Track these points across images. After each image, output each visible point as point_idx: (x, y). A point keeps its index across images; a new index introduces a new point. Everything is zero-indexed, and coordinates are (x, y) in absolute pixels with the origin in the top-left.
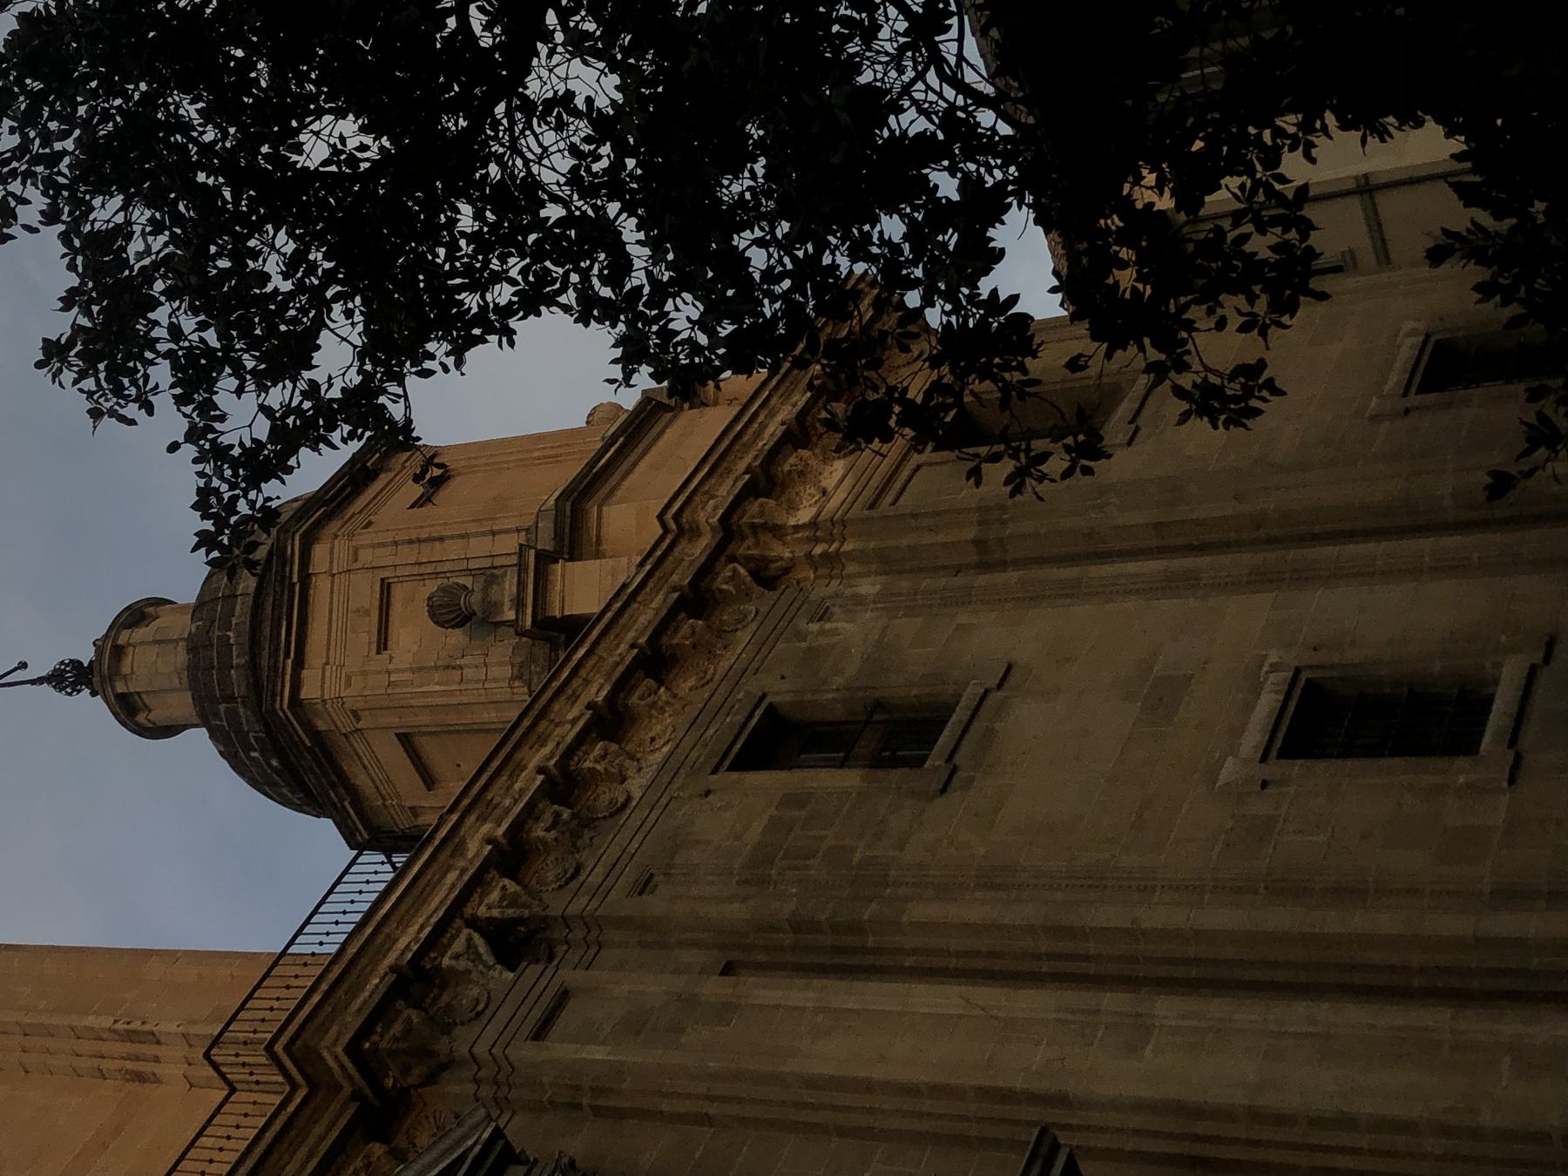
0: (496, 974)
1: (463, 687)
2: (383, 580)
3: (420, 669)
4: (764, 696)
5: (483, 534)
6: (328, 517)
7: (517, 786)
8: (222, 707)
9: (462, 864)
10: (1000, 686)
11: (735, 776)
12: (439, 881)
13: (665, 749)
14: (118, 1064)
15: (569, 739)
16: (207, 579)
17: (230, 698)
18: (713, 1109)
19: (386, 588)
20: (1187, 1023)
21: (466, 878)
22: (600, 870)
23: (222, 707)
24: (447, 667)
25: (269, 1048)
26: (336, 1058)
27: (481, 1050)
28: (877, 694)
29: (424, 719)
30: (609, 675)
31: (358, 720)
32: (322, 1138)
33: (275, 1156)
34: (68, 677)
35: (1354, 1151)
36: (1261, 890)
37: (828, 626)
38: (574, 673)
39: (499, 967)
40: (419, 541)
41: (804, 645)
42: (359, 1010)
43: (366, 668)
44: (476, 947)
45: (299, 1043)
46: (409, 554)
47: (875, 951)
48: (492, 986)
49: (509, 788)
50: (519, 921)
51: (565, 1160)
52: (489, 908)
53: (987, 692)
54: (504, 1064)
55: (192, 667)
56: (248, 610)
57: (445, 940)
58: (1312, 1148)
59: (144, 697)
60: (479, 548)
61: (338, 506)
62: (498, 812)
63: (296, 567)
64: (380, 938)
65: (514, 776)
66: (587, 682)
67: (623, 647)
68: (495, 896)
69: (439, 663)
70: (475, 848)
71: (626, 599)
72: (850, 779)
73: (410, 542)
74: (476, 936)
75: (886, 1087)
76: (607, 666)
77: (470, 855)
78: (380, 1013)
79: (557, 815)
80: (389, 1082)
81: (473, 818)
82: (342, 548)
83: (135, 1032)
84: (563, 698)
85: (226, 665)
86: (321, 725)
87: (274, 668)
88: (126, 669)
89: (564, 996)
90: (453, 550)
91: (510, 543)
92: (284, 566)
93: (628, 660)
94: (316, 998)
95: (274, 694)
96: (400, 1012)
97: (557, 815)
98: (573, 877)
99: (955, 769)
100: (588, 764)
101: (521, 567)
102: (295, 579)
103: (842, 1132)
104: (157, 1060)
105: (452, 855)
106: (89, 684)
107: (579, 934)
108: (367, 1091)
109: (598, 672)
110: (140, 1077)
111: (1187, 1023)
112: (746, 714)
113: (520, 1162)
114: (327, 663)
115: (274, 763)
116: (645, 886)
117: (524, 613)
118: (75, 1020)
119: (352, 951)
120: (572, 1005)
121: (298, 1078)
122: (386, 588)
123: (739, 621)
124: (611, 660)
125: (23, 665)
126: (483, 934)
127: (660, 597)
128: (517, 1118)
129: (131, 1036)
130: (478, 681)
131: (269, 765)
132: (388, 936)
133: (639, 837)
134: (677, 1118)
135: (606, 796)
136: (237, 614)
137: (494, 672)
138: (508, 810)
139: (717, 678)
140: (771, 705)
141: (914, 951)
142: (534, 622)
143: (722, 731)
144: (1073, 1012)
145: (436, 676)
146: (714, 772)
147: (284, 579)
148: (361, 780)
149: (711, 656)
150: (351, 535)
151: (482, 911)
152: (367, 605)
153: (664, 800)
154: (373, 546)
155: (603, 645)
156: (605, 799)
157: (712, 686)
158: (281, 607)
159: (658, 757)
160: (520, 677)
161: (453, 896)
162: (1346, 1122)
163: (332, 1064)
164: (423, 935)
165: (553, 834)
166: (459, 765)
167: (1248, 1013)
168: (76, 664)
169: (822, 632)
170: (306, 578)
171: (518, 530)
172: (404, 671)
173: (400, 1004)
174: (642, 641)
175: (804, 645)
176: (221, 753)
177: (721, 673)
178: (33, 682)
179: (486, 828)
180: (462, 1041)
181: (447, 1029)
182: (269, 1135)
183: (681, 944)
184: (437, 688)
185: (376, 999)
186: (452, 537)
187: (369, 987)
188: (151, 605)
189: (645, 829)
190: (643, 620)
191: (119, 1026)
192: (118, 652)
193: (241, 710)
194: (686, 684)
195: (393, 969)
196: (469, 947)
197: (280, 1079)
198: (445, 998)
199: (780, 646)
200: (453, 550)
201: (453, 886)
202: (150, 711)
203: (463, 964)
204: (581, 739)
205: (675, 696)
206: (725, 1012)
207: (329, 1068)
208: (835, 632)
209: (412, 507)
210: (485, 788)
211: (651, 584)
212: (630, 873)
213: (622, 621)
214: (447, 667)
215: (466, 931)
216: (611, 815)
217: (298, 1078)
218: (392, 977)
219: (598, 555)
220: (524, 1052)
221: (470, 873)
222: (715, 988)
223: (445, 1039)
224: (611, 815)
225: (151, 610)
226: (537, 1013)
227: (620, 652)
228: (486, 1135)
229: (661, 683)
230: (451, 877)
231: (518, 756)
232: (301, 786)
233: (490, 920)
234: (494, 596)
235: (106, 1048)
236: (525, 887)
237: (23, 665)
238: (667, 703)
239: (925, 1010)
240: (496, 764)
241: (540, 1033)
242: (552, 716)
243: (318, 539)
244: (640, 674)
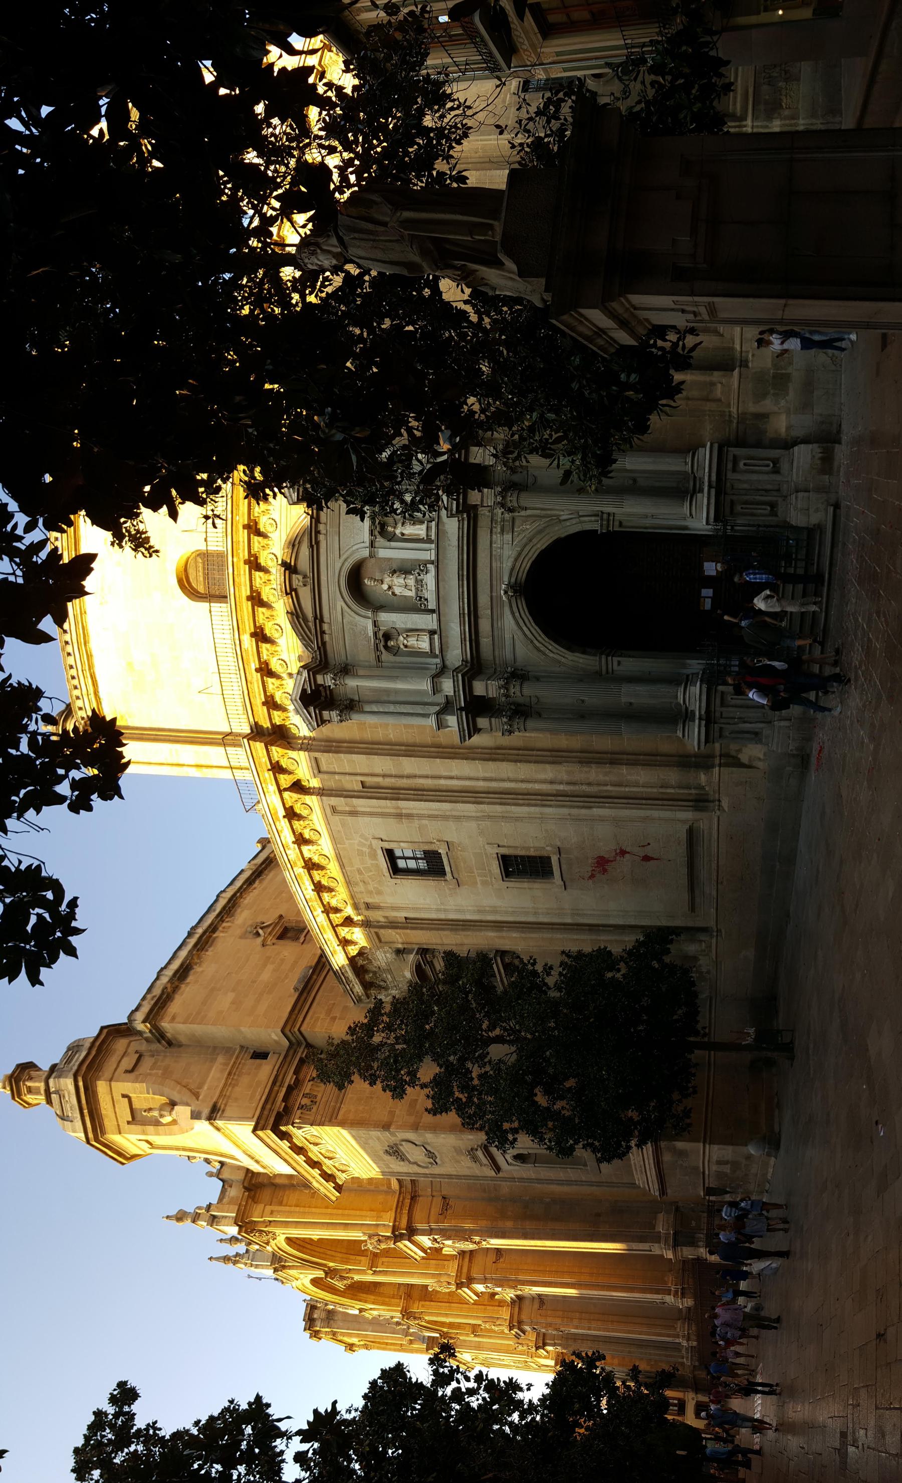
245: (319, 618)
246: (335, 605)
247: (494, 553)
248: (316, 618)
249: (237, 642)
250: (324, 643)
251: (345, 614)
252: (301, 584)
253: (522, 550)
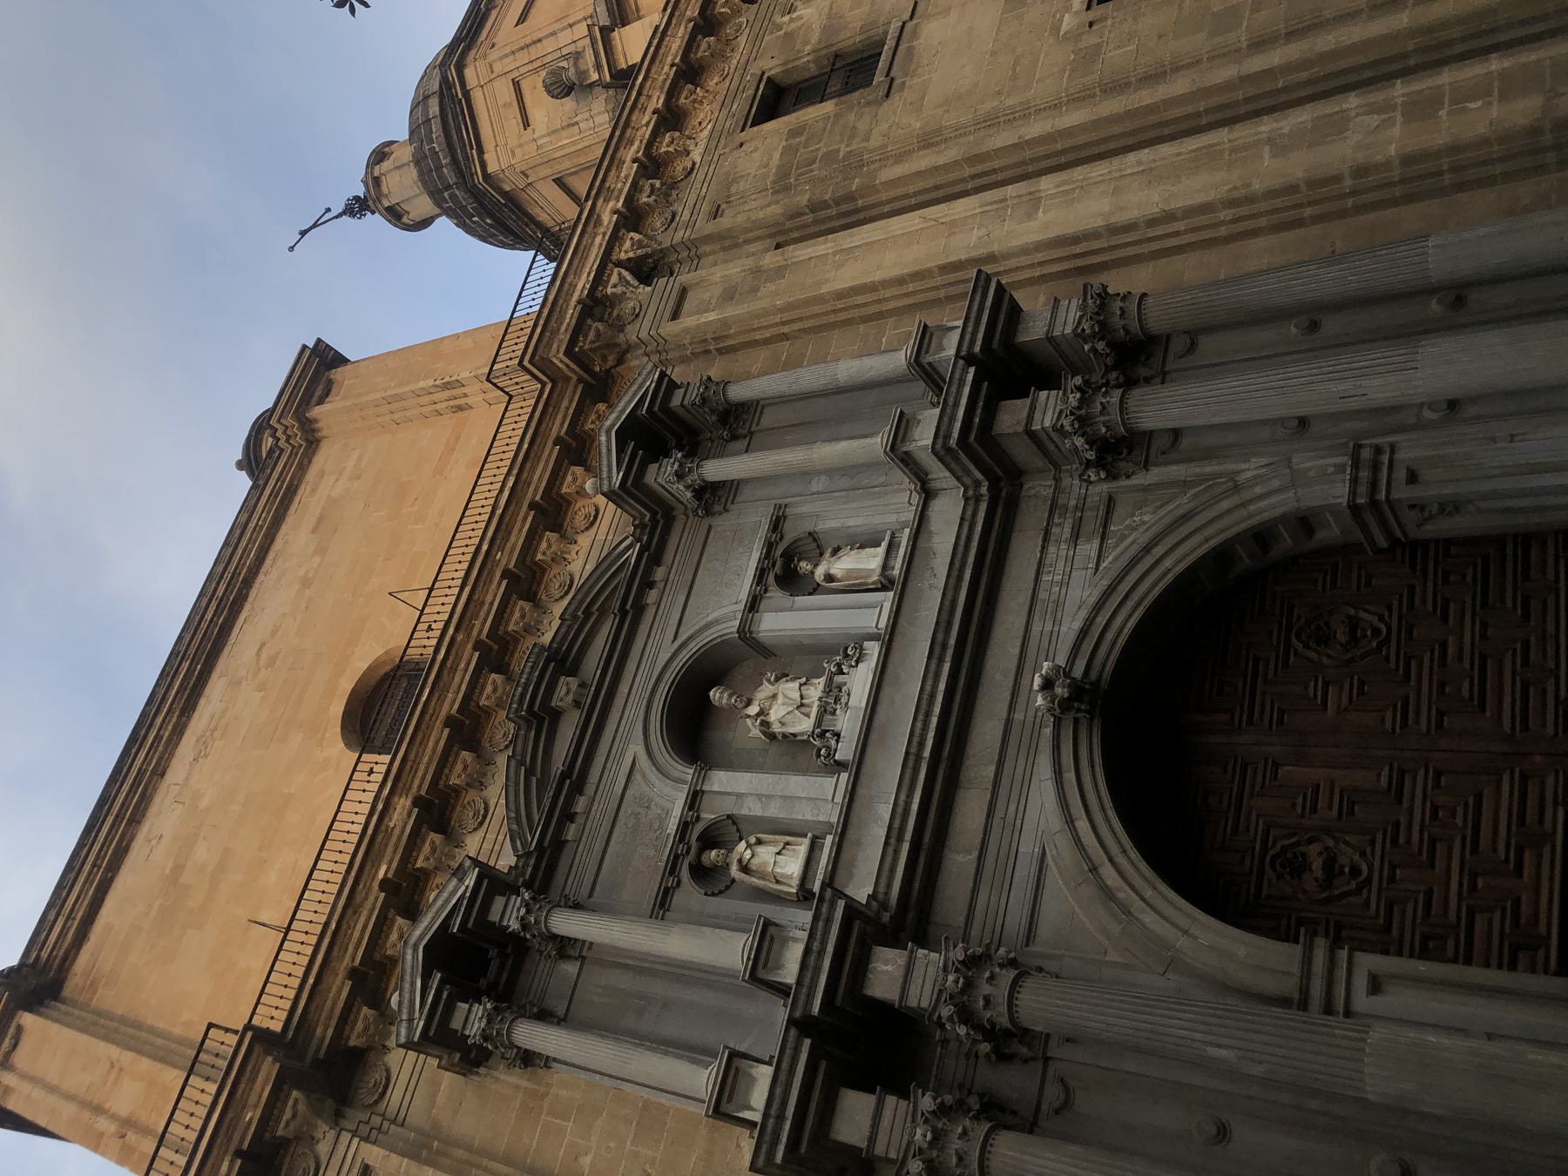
0: (640, 290)
1: (582, 136)
2: (513, 80)
3: (554, 132)
4: (763, 73)
5: (563, 29)
6: (468, 48)
7: (623, 175)
8: (446, 194)
9: (602, 230)
10: (911, 18)
11: (755, 129)
12: (592, 243)
13: (709, 126)
14: (446, 404)
15: (647, 136)
16: (411, 112)
17: (448, 187)
18: (786, 329)
19: (516, 85)
20: (1062, 189)
21: (607, 237)
22: (687, 213)
23: (446, 194)
24: (569, 126)
25: (520, 364)
26: (561, 361)
27: (643, 335)
28: (835, 48)
29: (567, 164)
30: (662, 88)
31: (527, 177)
32: (568, 408)
33: (544, 425)
34: (357, 208)
35: (1177, 234)
36: (1099, 93)
37: (794, 15)
38: (639, 94)
39: (642, 286)
40: (527, 46)
41: (781, 33)
42: (566, 330)
43: (522, 141)
44: (625, 278)
45: (537, 358)
46: (523, 57)
47: (864, 208)
48: (640, 298)
49: (618, 177)
50: (647, 256)
51: (705, 378)
52: (626, 252)
53: (904, 23)
54: (660, 340)
55: (421, 174)
56: (440, 126)
57: (605, 278)
58: (1150, 240)
59: (402, 205)
60: (565, 38)
61: (472, 39)
62: (616, 193)
63: (458, 88)
64: (566, 285)
65: (619, 168)
66: (649, 97)
67: (666, 68)
68: (628, 244)
69: (564, 125)
70: (608, 219)
71: (660, 36)
72: (828, 107)
73: (522, 49)
74: (623, 271)
75: (885, 284)
76: (659, 82)
77: (605, 224)
78: (579, 330)
79: (652, 186)
80: (597, 369)
81: (601, 200)
82: (481, 65)
83: (448, 383)
84: (637, 112)
85: (439, 167)
86: (507, 188)
87: (466, 157)
88: (385, 191)
89: (683, 292)
90: (549, 46)
91: (582, 29)
92: (451, 89)
93: (671, 77)
94: (539, 330)
95: (472, 175)
96: (590, 327)
97: (652, 186)
98: (672, 221)
99: (892, 79)
100: (663, 150)
101: (593, 43)
102: (460, 96)
103: (866, 319)
104: (466, 395)
105: (595, 227)
106: (368, 208)
107: (685, 254)
108: (586, 376)
109: (654, 88)
110: (460, 408)
111: (1062, 189)
112: (754, 88)
113: (679, 387)
114: (497, 146)
115: (488, 221)
116: (716, 213)
117: (603, 71)
118: (412, 387)
119: (551, 297)
120: (690, 296)
121: (544, 378)
122: (516, 85)
123: (737, 31)
124: (661, 78)
125: (328, 210)
126: (626, 269)
127: (682, 28)
128: (676, 369)
129: (447, 386)
130: (590, 129)
131: (486, 223)
132: (571, 284)
133: (706, 185)
134: (767, 342)
135: (680, 166)
137: (598, 120)
138: (621, 191)
139: (731, 71)
140: (768, 77)
141: (889, 202)
142: (611, 76)
143: (739, 106)
144: (990, 204)
145: (564, 133)
146: (742, 130)
147: (453, 97)
148: (543, 217)
149: (725, 59)
150: (485, 56)
151: (623, 256)
152: (509, 100)
153: (716, 158)
154: (500, 59)
155: (653, 70)
156: (679, 168)
157: (730, 77)
158: (457, 117)
159: (706, 133)
161: (602, 251)
162: (1169, 217)
163: (560, 365)
164: (591, 278)
165: (653, 197)
167: (1099, 170)
168: (357, 198)
169: (792, 20)
170: (467, 94)
171: (585, 19)
172: (544, 136)
173: (589, 321)
174: (677, 61)
175: (781, 33)
176: (457, 225)
177: (733, 67)
178: (336, 217)
179: (611, 204)
180: (631, 334)
181: (621, 329)
182: (537, 414)
183: (747, 242)
184: (568, 141)
185: (574, 321)
186: (547, 37)
187: (568, 316)
188: (387, 146)
189: (708, 179)
190: (675, 47)
191: (438, 382)
192: (377, 181)
193: (457, 192)
194: (712, 82)
195: (579, 302)
196: (620, 279)
197: (529, 377)
198: (615, 313)
199: (766, 38)
200: (549, 46)
201: (601, 245)
202: (408, 213)
203: (619, 290)
204: (655, 134)
205: (707, 91)
206: (779, 272)
207: (559, 368)
208: (800, 17)
209: (516, 25)
210: (604, 181)
211: (674, 22)
212: (706, 207)
213: (661, 52)
214: (569, 126)
215: (616, 270)
216: (686, 177)
217: (544, 378)
218: (579, 308)
219: (640, 18)
220: (669, 329)
221: (609, 234)
222: (771, 259)
223: (621, 335)
224: (686, 177)
225: (387, 149)
226: (671, 303)
227: (665, 72)
228: (656, 376)
229: (697, 86)
230: (598, 240)
231: (619, 155)
232: (507, 231)
233: (629, 259)
234: (582, 68)
235: (435, 397)
236: (645, 236)
237: (328, 210)
238: (704, 97)
239: (900, 232)
240: (606, 163)
241: (675, 316)
242: (633, 124)
243: (465, 65)
244: (682, 83)
245: (576, 779)
246: (623, 754)
247: (1042, 595)
248: (566, 775)
249: (380, 806)
250: (559, 844)
251: (637, 776)
252: (570, 698)
253: (1119, 579)
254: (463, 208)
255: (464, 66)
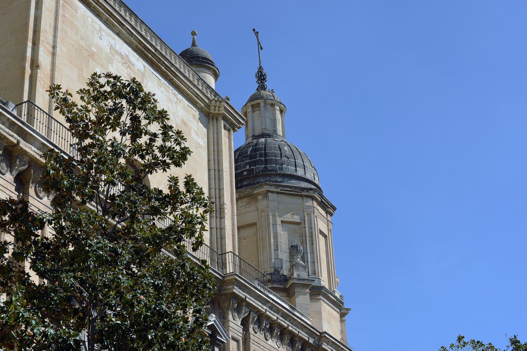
115: (245, 173)
125: (262, 49)
136: (291, 167)
160: (275, 270)
166: (245, 239)
170: (302, 196)
193: (263, 166)
195: (246, 297)
237: (262, 49)
254: (255, 163)
255: (313, 200)
